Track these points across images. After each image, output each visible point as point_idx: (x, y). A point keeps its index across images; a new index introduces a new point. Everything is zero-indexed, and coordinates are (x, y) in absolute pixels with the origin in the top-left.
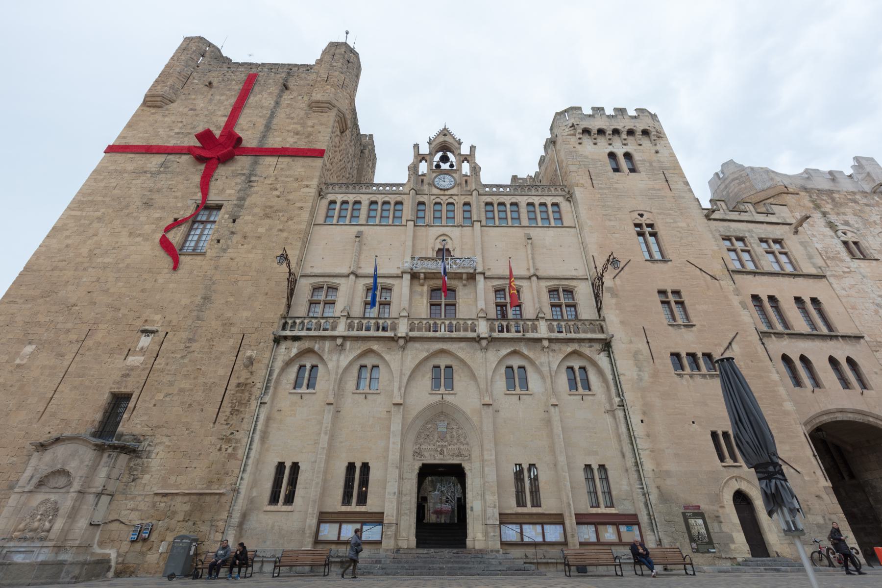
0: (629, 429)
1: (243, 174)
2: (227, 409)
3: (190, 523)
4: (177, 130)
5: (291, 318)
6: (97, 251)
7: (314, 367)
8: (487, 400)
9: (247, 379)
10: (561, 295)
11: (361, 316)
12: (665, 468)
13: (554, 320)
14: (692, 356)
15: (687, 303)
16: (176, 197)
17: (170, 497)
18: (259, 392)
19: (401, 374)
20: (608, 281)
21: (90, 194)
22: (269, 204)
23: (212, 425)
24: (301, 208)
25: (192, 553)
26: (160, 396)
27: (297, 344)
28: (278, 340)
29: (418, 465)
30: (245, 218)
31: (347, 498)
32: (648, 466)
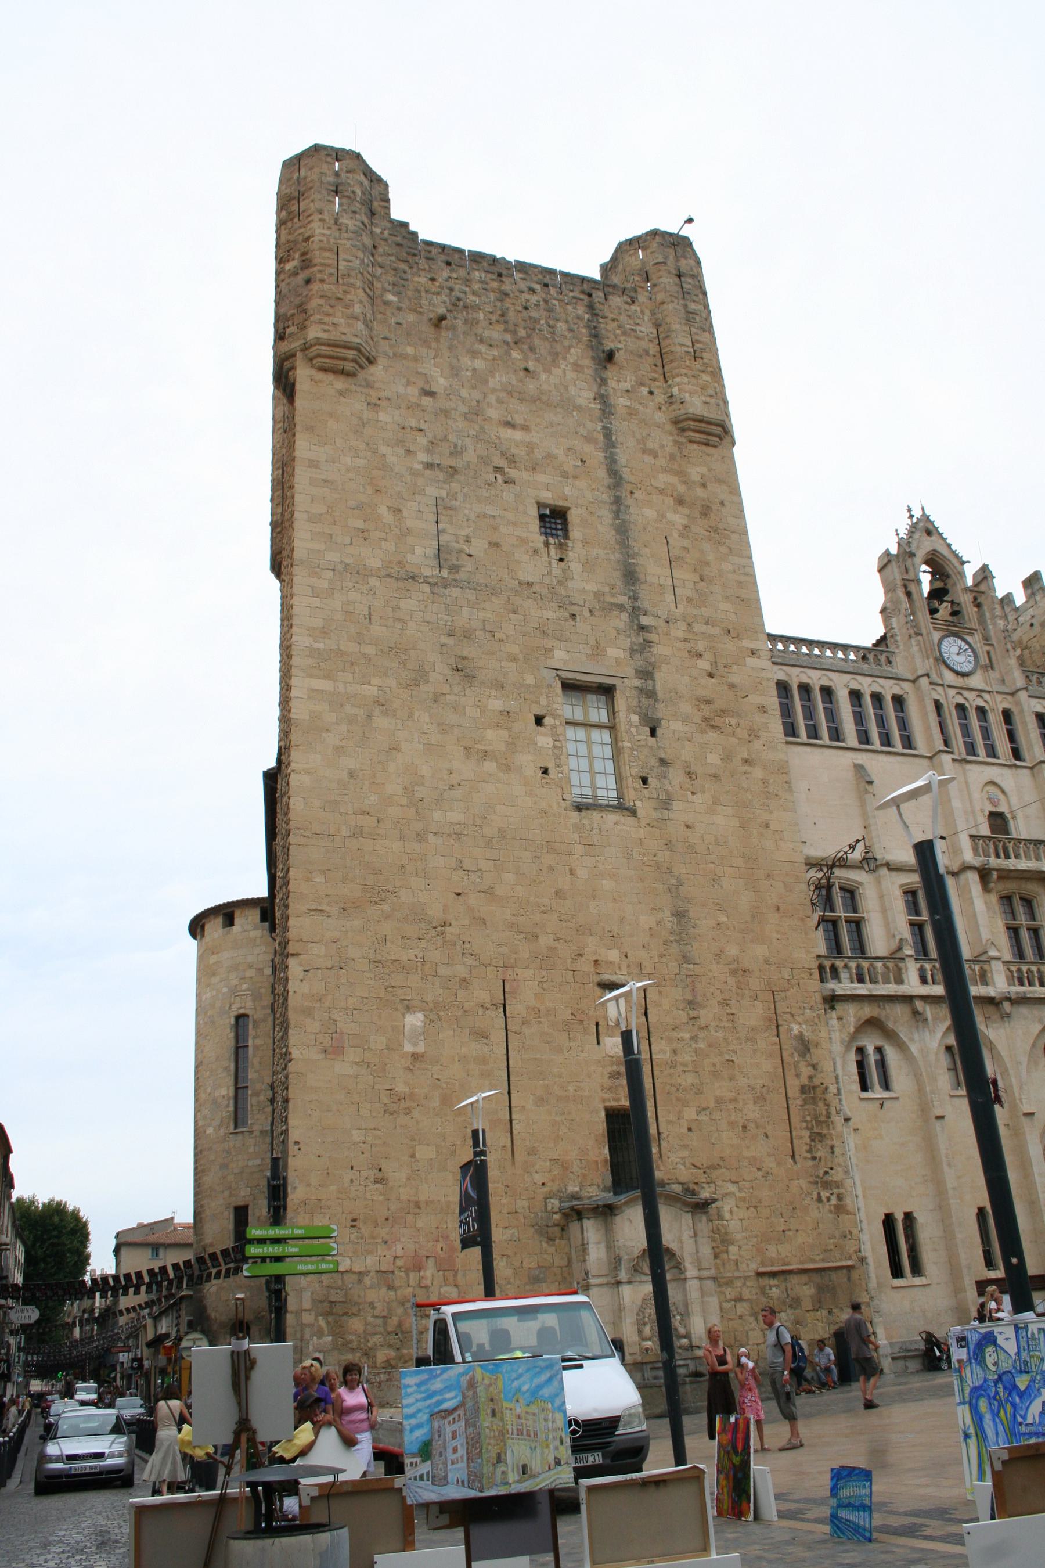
1: (621, 607)
2: (803, 1136)
3: (825, 1312)
4: (423, 457)
6: (421, 792)
16: (513, 659)
17: (782, 1278)
24: (763, 709)
26: (690, 1113)
30: (671, 727)
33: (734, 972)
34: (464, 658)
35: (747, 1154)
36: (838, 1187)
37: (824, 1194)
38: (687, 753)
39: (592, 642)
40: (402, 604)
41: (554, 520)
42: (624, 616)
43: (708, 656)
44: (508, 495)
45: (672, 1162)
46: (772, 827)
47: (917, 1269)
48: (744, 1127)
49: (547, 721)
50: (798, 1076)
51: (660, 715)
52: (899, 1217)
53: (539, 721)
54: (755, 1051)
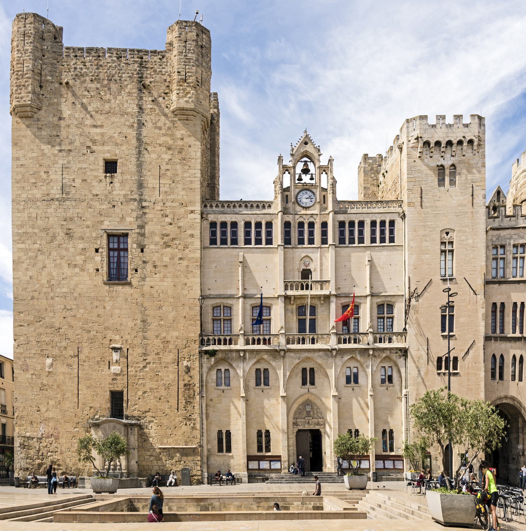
1: (135, 200)
2: (182, 401)
5: (205, 336)
7: (227, 370)
16: (88, 227)
21: (22, 226)
22: (164, 232)
24: (192, 236)
30: (150, 247)
34: (70, 229)
38: (155, 257)
39: (121, 216)
40: (48, 211)
41: (111, 167)
42: (136, 203)
43: (171, 216)
44: (92, 158)
45: (131, 409)
46: (188, 285)
48: (160, 399)
49: (100, 250)
51: (145, 243)
53: (97, 251)
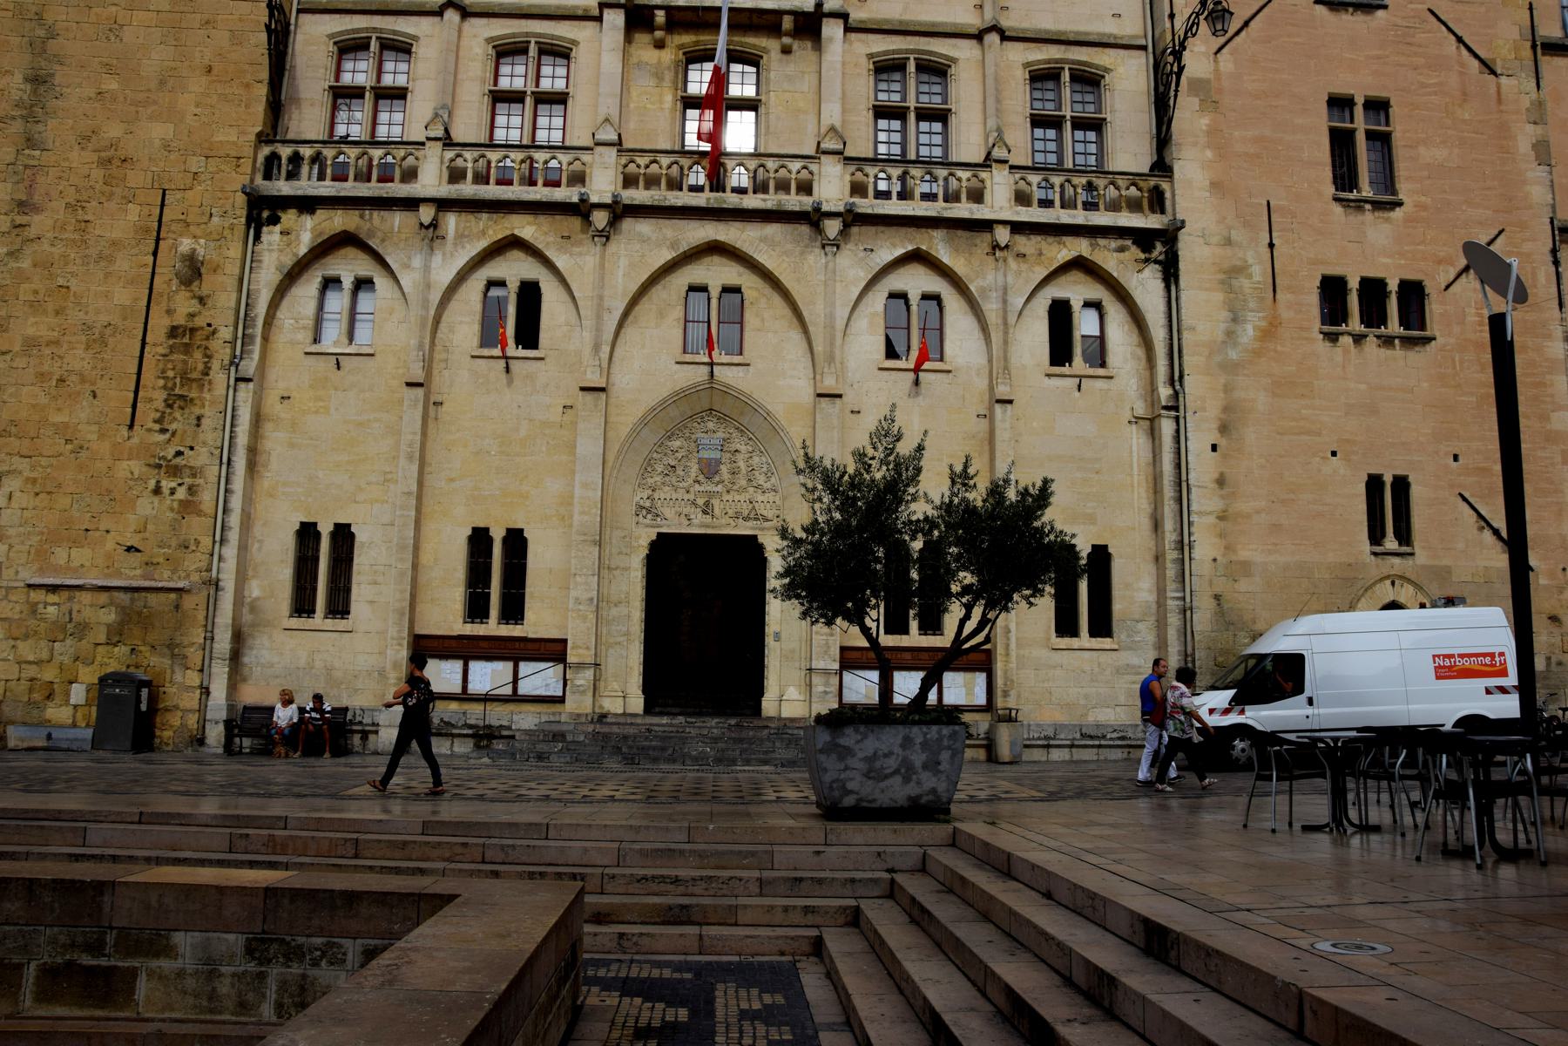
0: (1178, 466)
2: (155, 395)
8: (829, 384)
9: (192, 315)
10: (1067, 92)
11: (482, 138)
12: (1243, 554)
13: (1034, 169)
14: (1373, 290)
15: (1398, 140)
17: (65, 594)
18: (228, 351)
19: (600, 310)
20: (1198, 60)
23: (124, 431)
25: (144, 707)
27: (308, 222)
28: (262, 211)
29: (645, 536)
31: (476, 608)
32: (1205, 548)
33: (106, 163)
35: (58, 418)
36: (194, 476)
37: (167, 484)
47: (339, 607)
50: (169, 312)
52: (325, 529)
54: (107, 275)
